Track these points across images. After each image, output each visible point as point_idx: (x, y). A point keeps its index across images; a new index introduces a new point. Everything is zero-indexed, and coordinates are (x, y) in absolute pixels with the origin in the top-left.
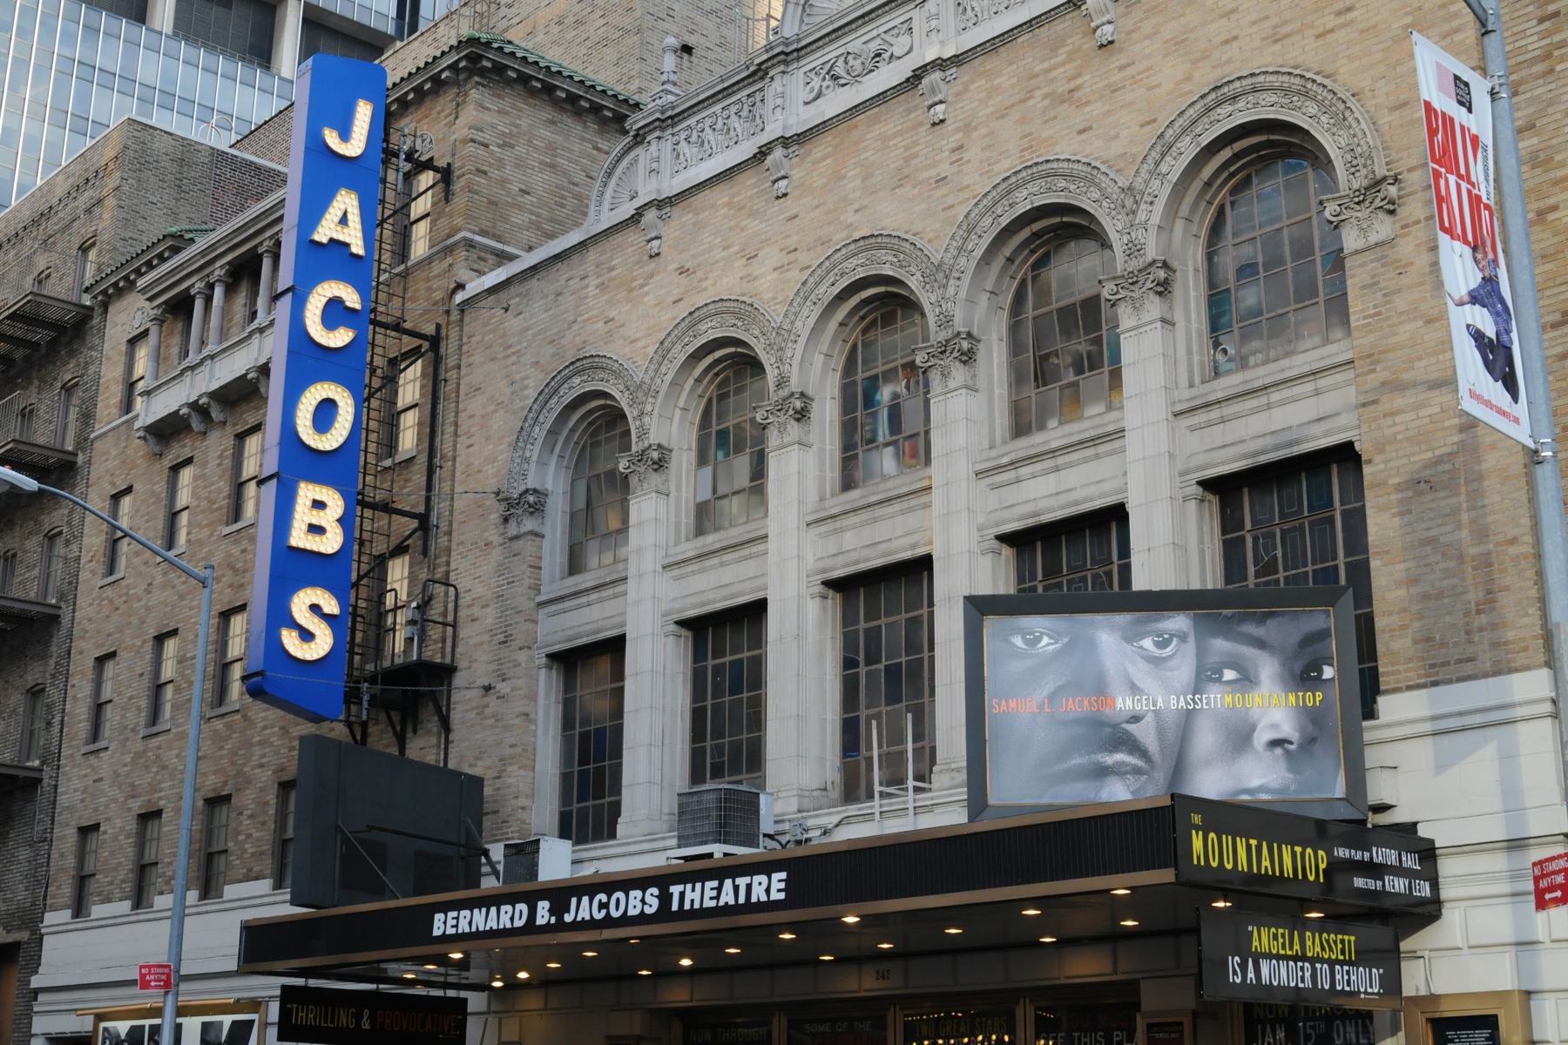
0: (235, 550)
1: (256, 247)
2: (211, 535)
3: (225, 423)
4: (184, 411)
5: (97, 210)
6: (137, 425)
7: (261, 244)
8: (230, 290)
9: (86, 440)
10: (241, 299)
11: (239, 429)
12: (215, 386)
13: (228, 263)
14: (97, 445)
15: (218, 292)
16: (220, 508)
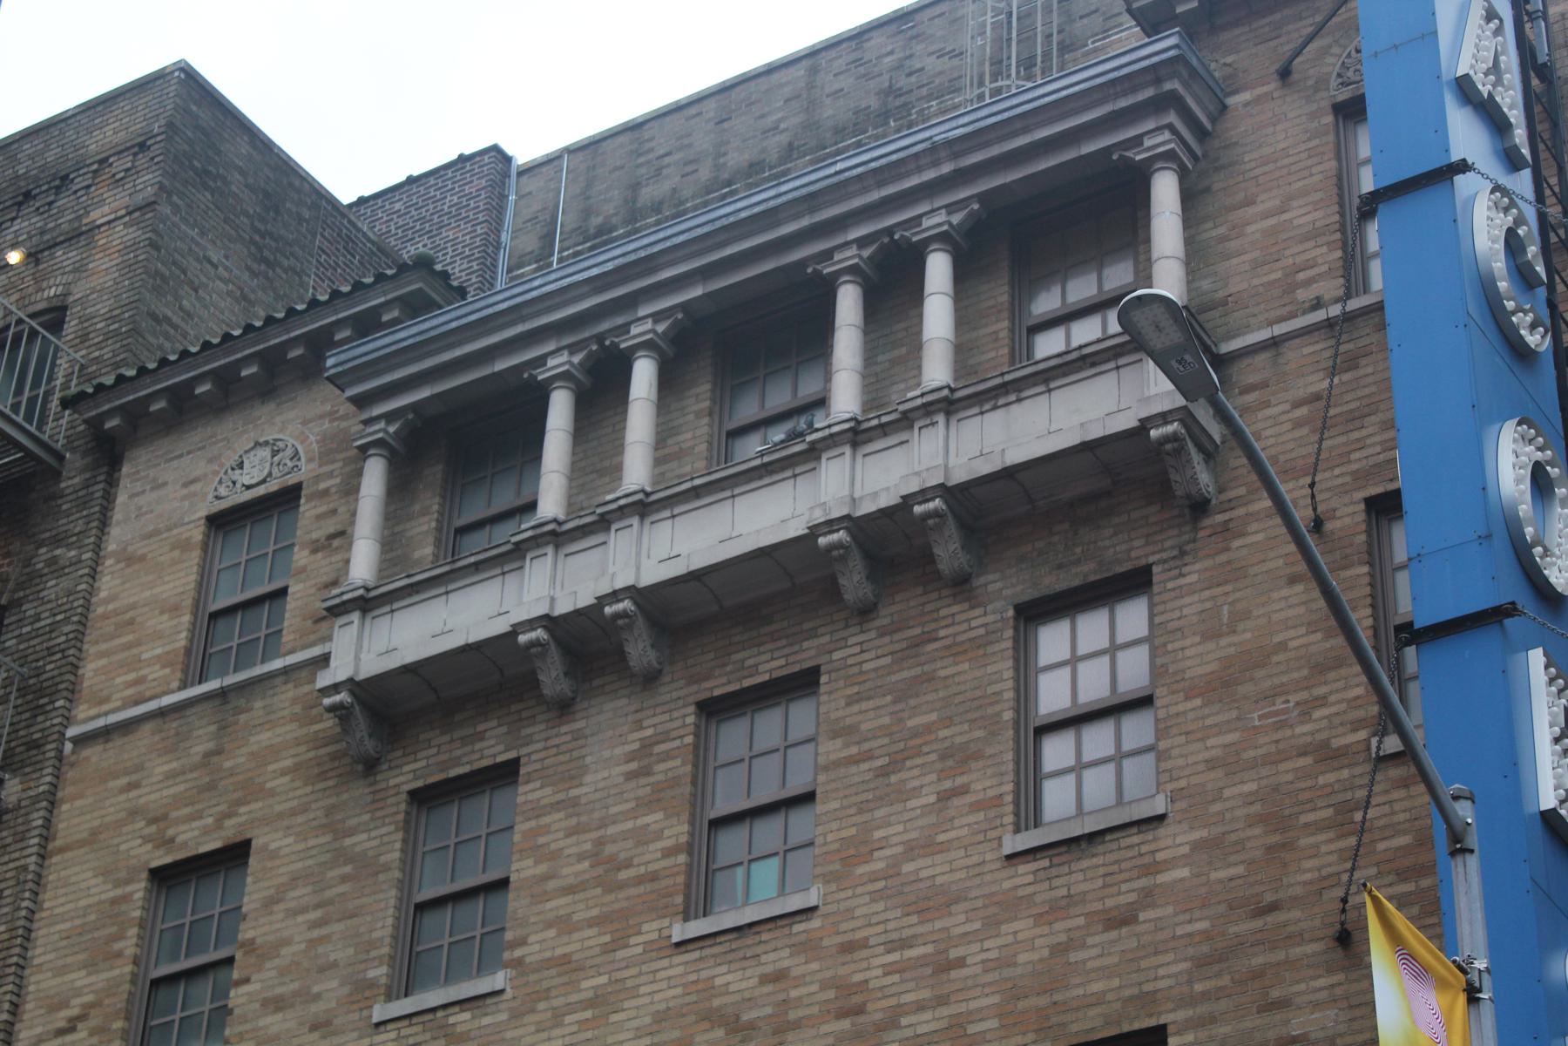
0: (734, 980)
1: (803, 263)
2: (619, 943)
3: (650, 679)
4: (539, 633)
5: (65, 257)
6: (325, 679)
7: (827, 255)
8: (667, 383)
9: (35, 745)
10: (700, 396)
11: (720, 686)
12: (652, 574)
13: (683, 306)
14: (93, 753)
15: (644, 374)
16: (654, 877)
